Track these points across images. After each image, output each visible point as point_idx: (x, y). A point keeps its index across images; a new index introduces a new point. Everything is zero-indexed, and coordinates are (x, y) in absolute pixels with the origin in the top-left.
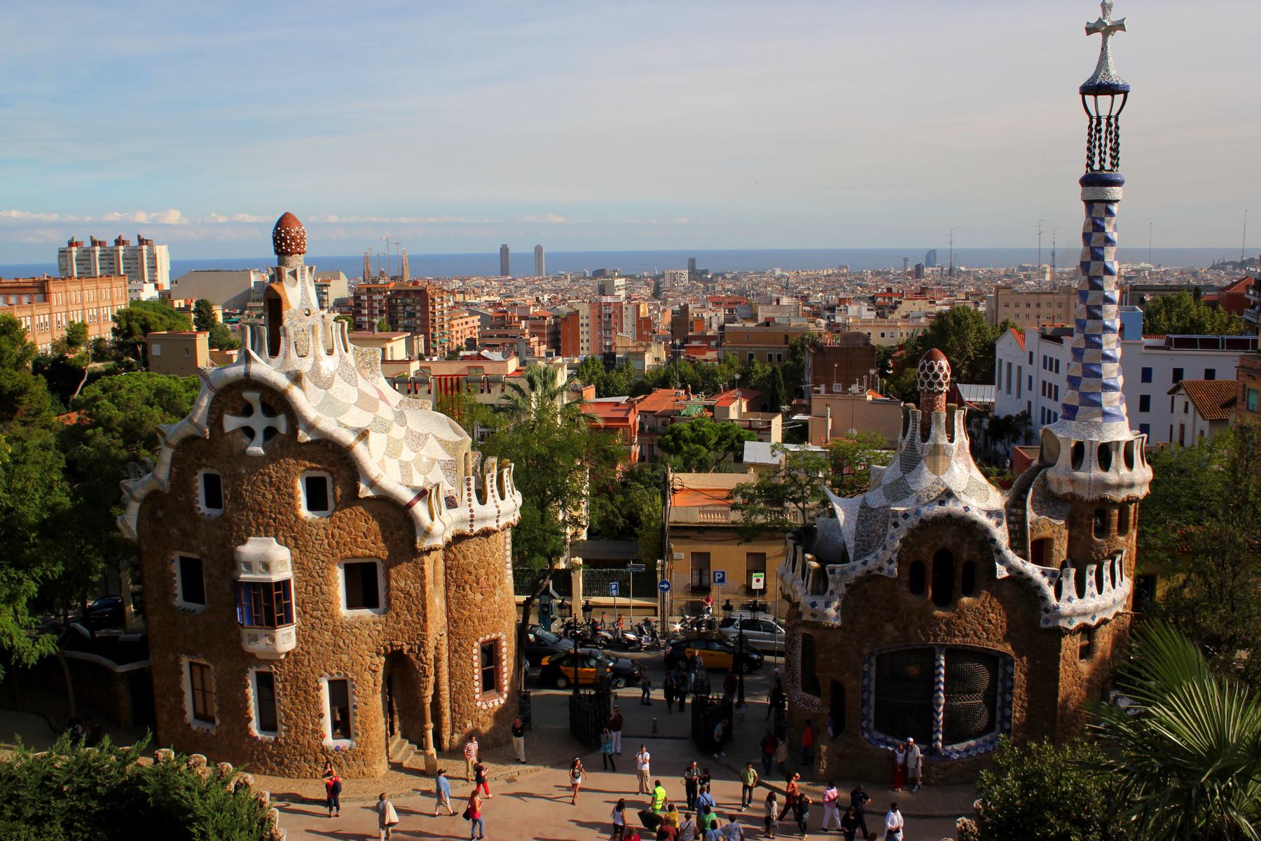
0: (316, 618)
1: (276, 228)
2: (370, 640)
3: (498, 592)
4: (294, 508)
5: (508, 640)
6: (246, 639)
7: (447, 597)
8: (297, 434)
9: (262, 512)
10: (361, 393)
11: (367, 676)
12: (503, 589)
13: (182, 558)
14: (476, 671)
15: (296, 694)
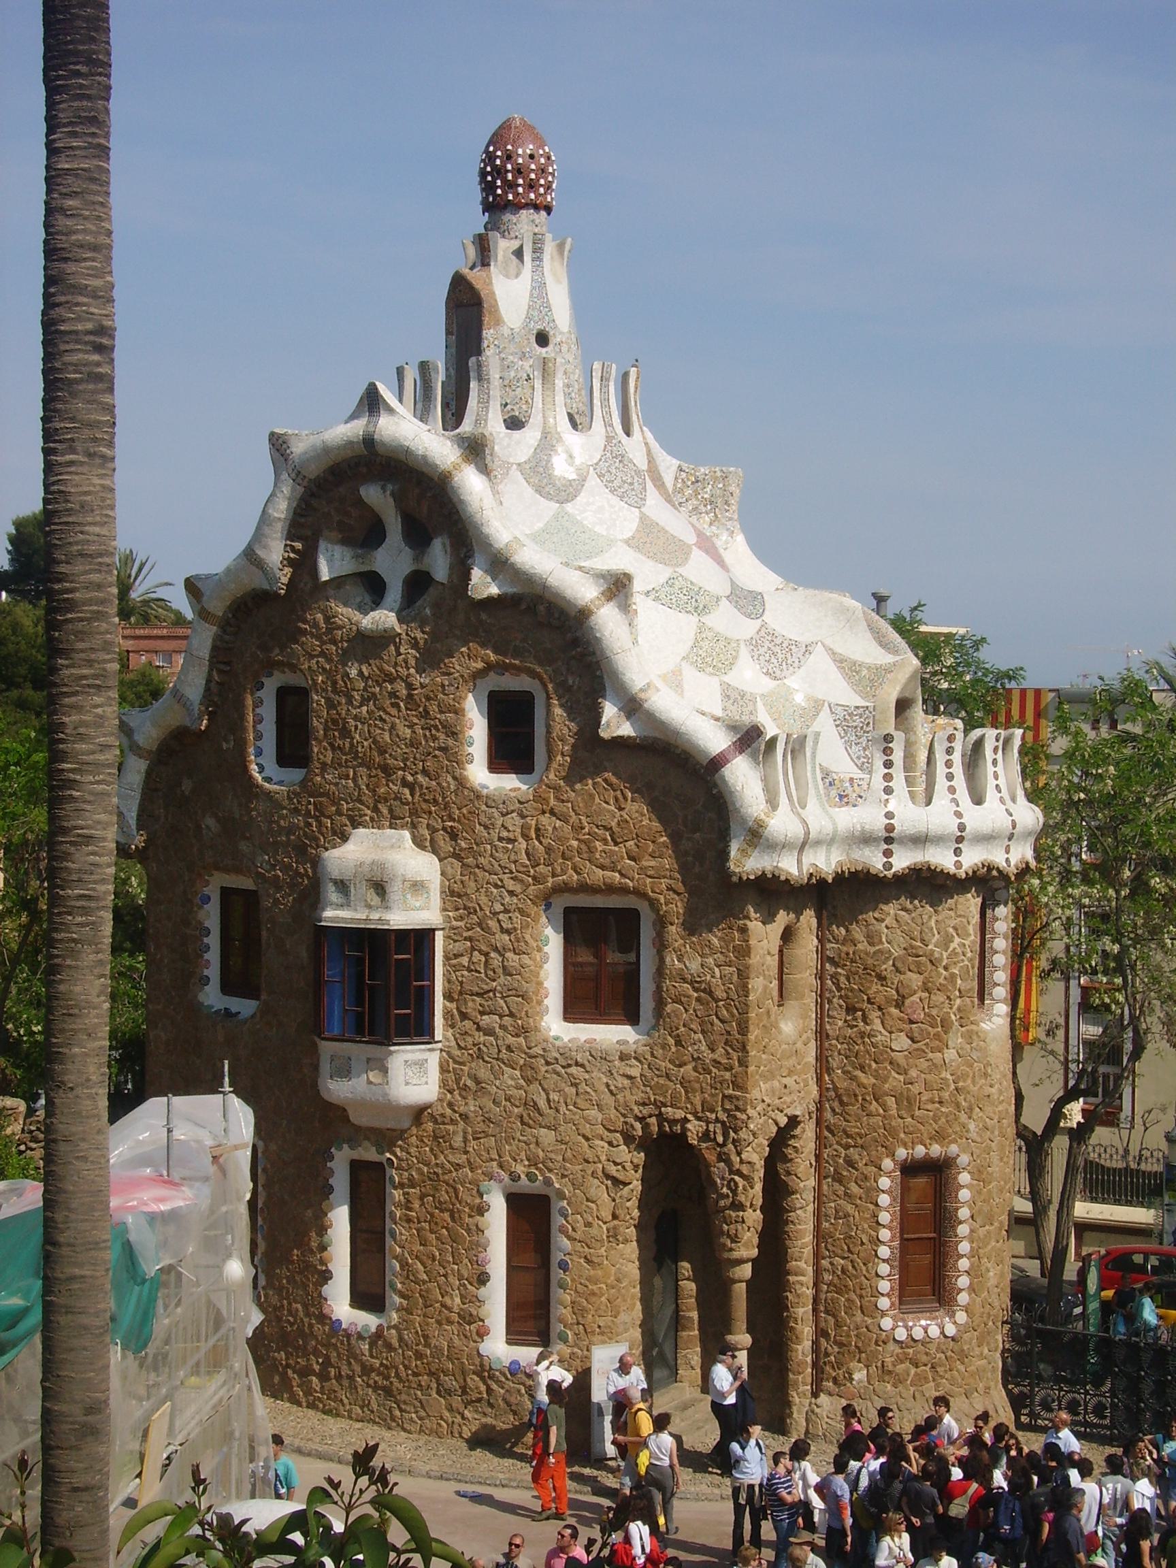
0: (489, 1032)
1: (486, 151)
2: (608, 1100)
3: (956, 1039)
4: (455, 758)
5: (979, 1175)
6: (325, 1067)
7: (821, 1035)
8: (467, 577)
9: (387, 770)
10: (646, 524)
11: (598, 1190)
12: (969, 1037)
13: (226, 893)
14: (885, 1234)
15: (432, 1220)
